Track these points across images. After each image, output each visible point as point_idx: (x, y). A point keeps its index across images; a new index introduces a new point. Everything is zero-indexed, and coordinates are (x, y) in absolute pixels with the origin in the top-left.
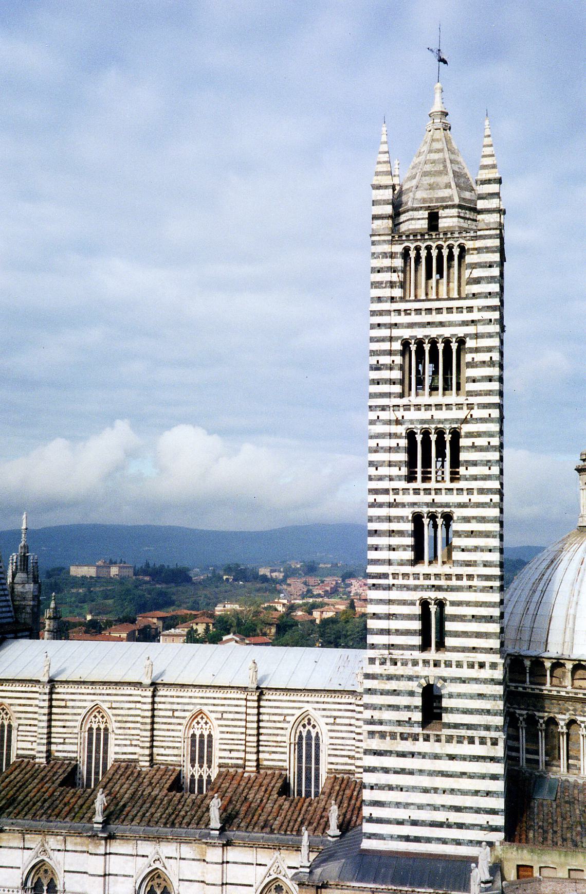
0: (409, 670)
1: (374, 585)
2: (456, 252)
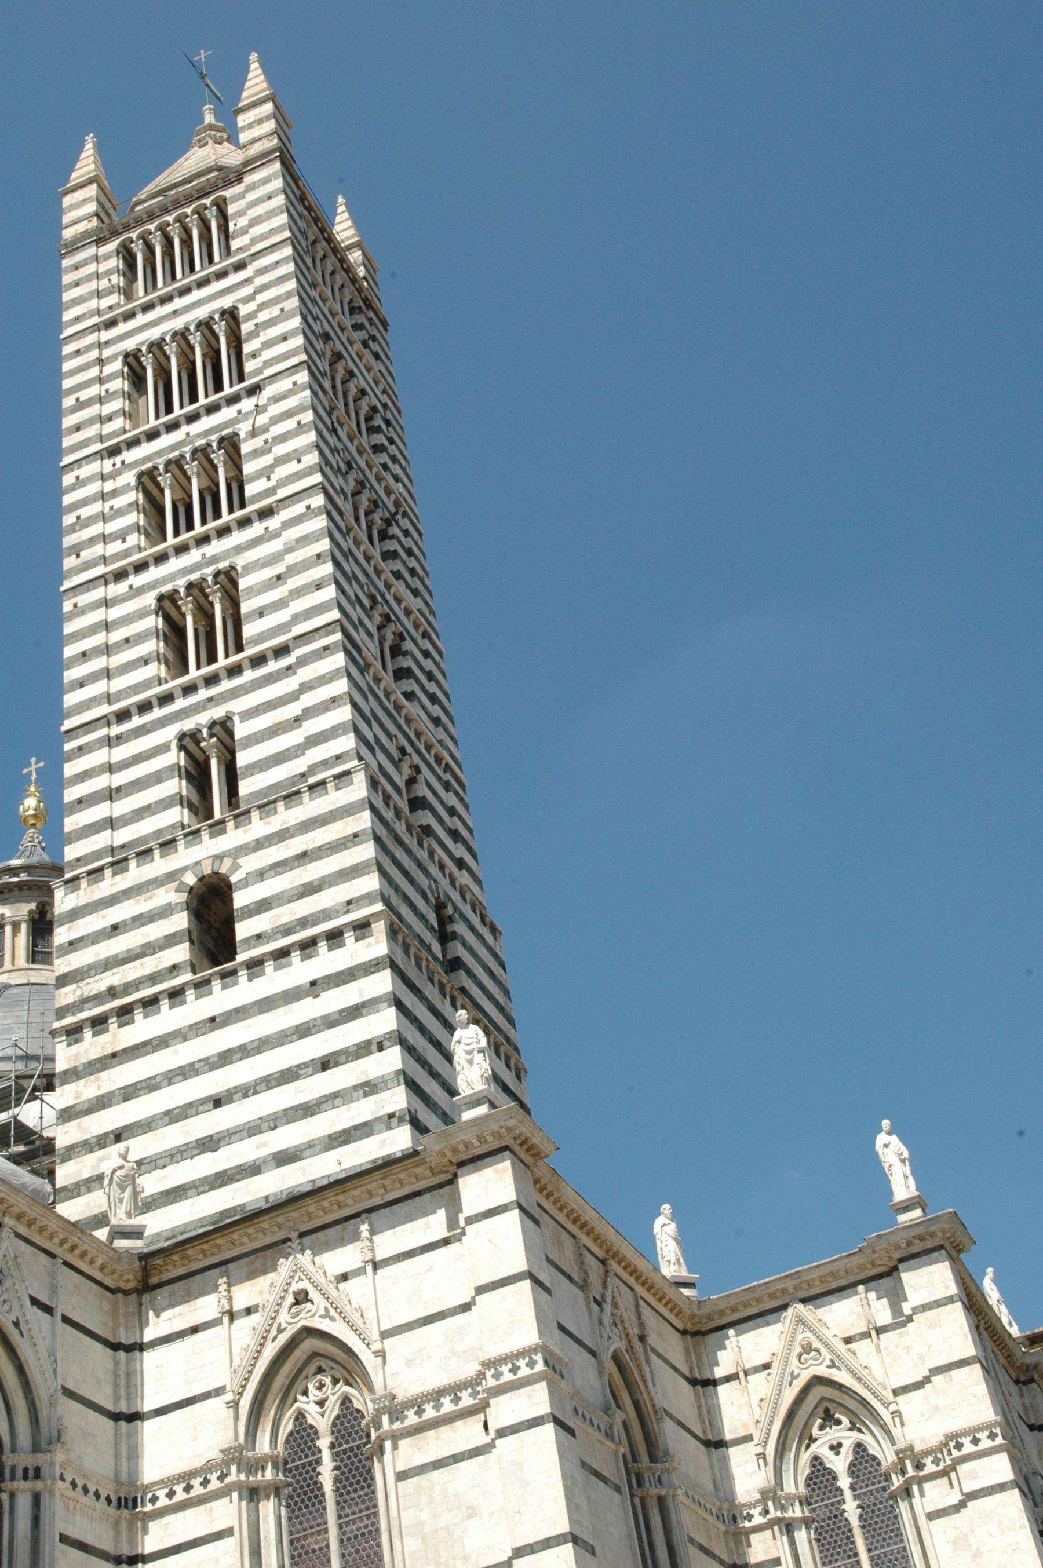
0: (160, 865)
1: (80, 748)
2: (212, 215)
